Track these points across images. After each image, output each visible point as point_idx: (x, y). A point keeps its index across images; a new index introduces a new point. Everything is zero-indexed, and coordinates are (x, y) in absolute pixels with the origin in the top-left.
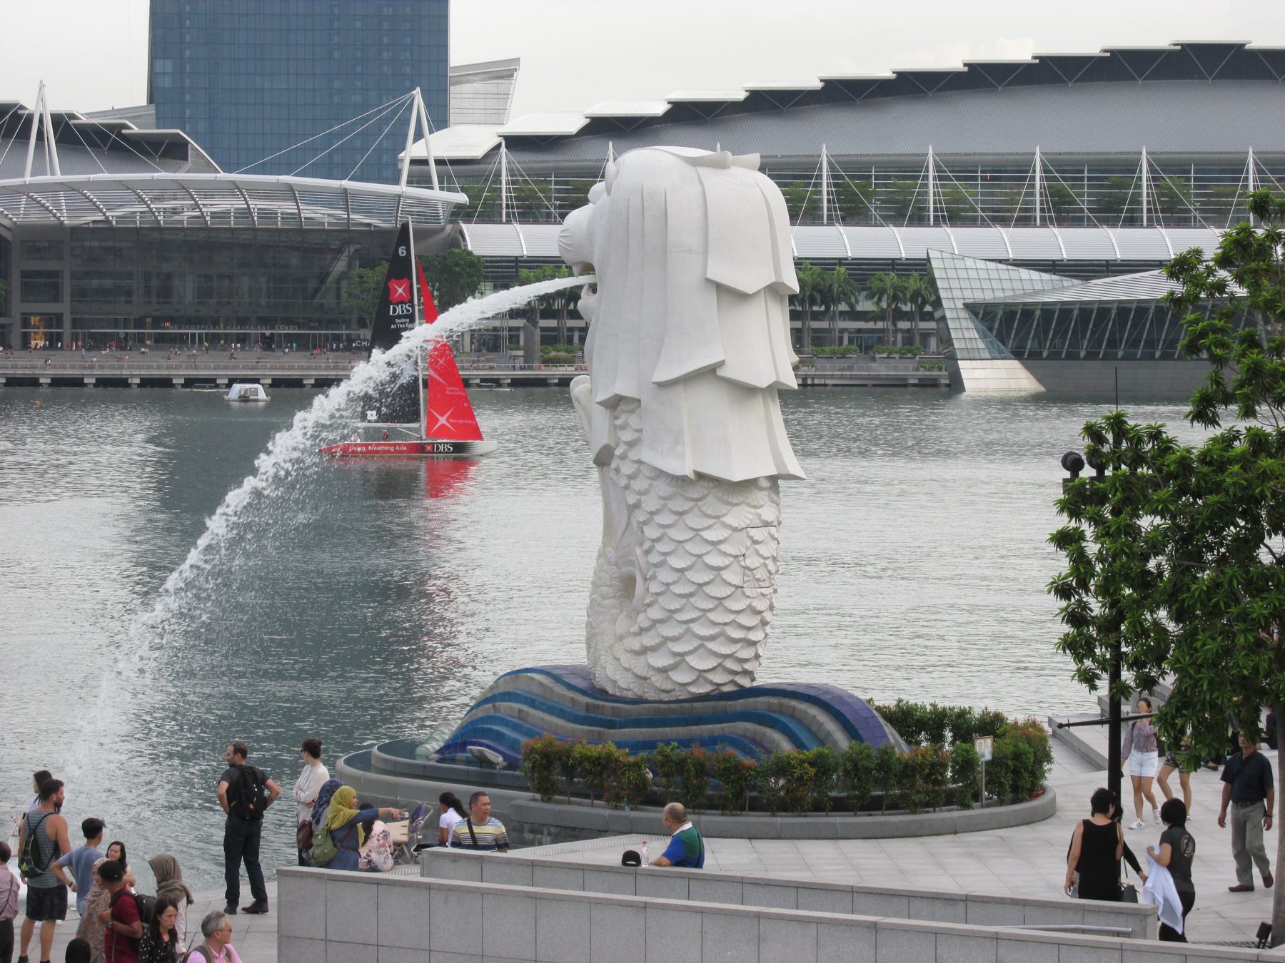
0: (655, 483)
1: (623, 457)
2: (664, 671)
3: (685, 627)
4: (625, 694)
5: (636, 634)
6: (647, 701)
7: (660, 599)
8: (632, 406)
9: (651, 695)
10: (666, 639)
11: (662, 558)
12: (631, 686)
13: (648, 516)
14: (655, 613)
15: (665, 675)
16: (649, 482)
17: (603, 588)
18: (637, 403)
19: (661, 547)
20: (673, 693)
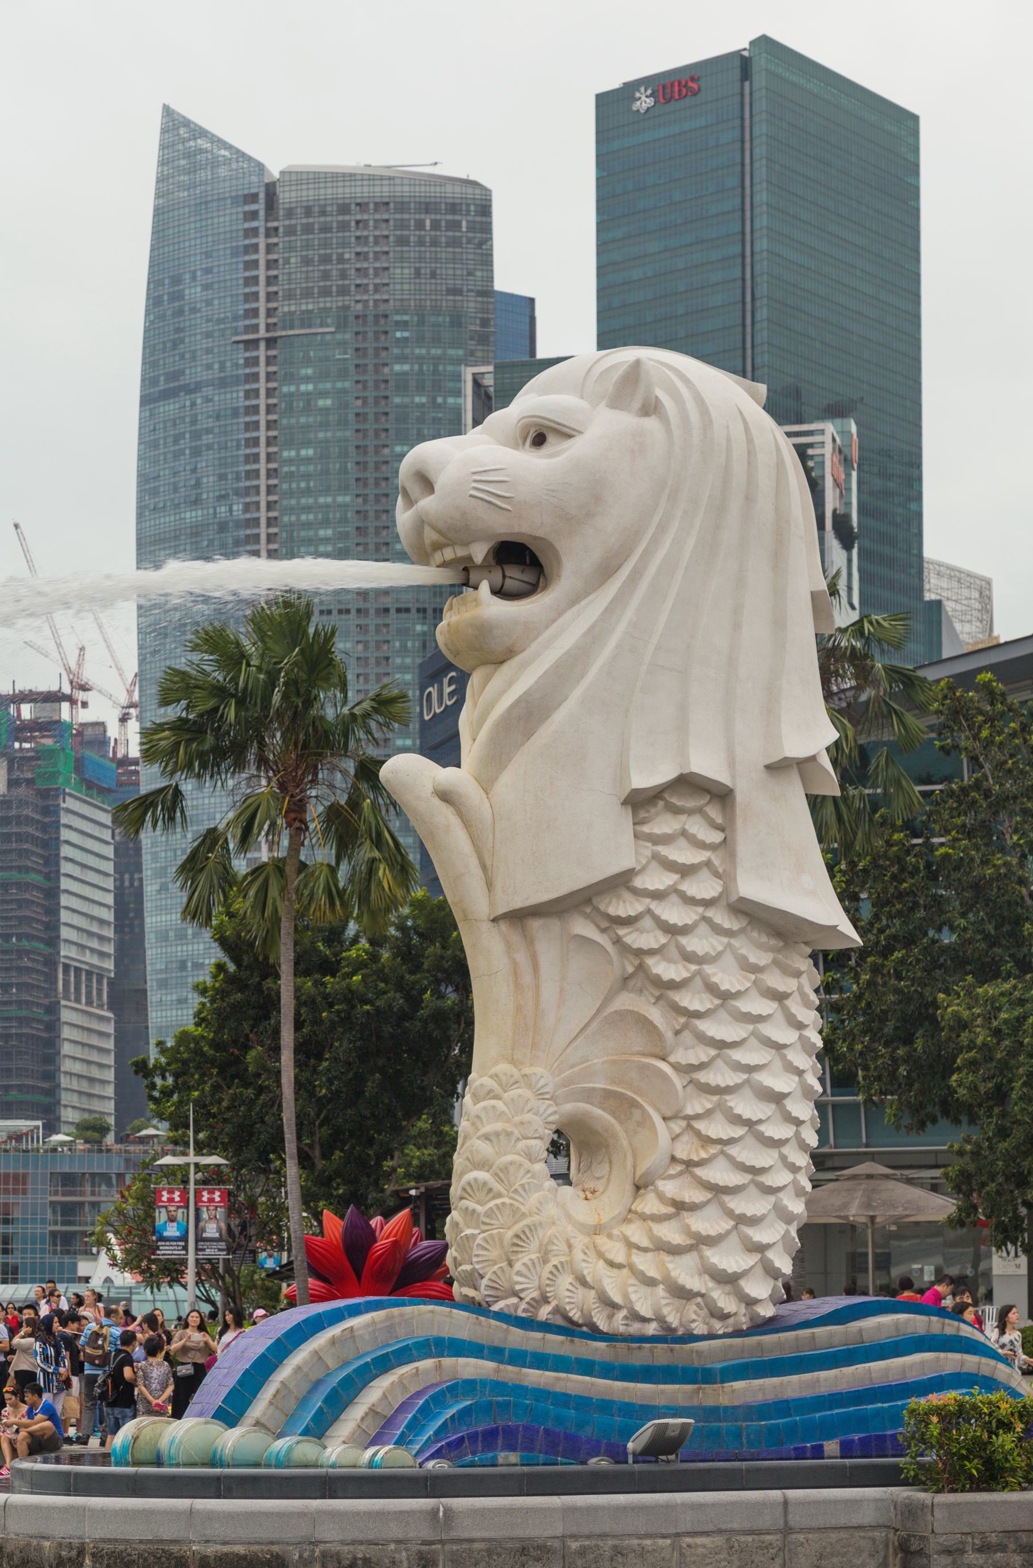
0: (734, 942)
2: (729, 1280)
3: (772, 1199)
4: (635, 1328)
6: (691, 1338)
7: (733, 1151)
8: (702, 802)
9: (699, 1328)
10: (742, 1220)
11: (745, 1076)
12: (665, 1311)
13: (717, 1002)
14: (720, 1174)
15: (728, 1288)
16: (726, 940)
18: (708, 797)
19: (738, 1055)
20: (731, 1320)
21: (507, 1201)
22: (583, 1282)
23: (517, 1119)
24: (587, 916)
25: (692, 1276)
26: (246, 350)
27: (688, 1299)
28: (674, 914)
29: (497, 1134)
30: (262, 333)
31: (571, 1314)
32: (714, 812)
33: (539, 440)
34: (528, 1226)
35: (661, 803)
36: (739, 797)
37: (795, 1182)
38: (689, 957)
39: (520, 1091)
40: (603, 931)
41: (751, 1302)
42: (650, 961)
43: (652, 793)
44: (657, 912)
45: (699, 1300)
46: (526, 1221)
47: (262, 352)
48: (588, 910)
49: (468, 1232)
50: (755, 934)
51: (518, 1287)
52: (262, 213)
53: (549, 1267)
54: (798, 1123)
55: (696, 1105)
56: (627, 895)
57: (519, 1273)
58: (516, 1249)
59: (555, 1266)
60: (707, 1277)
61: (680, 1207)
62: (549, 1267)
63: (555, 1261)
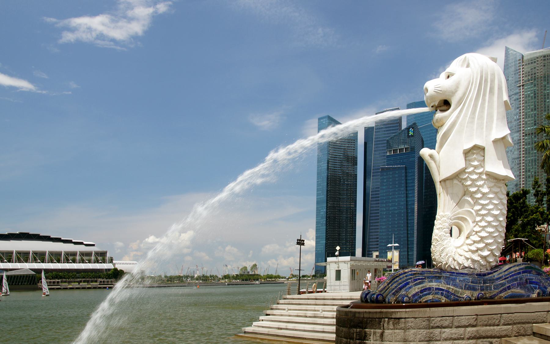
1: (470, 173)
5: (470, 245)
8: (479, 151)
10: (487, 244)
14: (483, 234)
15: (484, 259)
17: (446, 229)
19: (487, 207)
21: (440, 242)
22: (454, 260)
23: (443, 225)
24: (457, 179)
25: (476, 257)
26: (519, 87)
27: (476, 262)
28: (474, 177)
29: (439, 228)
30: (521, 84)
31: (451, 267)
32: (482, 153)
33: (448, 77)
34: (444, 248)
35: (471, 152)
36: (486, 149)
37: (500, 234)
38: (476, 186)
39: (444, 218)
40: (460, 182)
41: (490, 262)
42: (469, 187)
43: (468, 150)
44: (470, 176)
45: (478, 262)
46: (444, 247)
47: (521, 87)
48: (457, 177)
49: (433, 249)
50: (490, 179)
51: (442, 261)
52: (521, 62)
53: (447, 256)
54: (500, 221)
55: (478, 219)
56: (464, 173)
57: (442, 258)
58: (441, 253)
59: (449, 256)
60: (479, 257)
61: (475, 242)
62: (447, 256)
63: (449, 255)
